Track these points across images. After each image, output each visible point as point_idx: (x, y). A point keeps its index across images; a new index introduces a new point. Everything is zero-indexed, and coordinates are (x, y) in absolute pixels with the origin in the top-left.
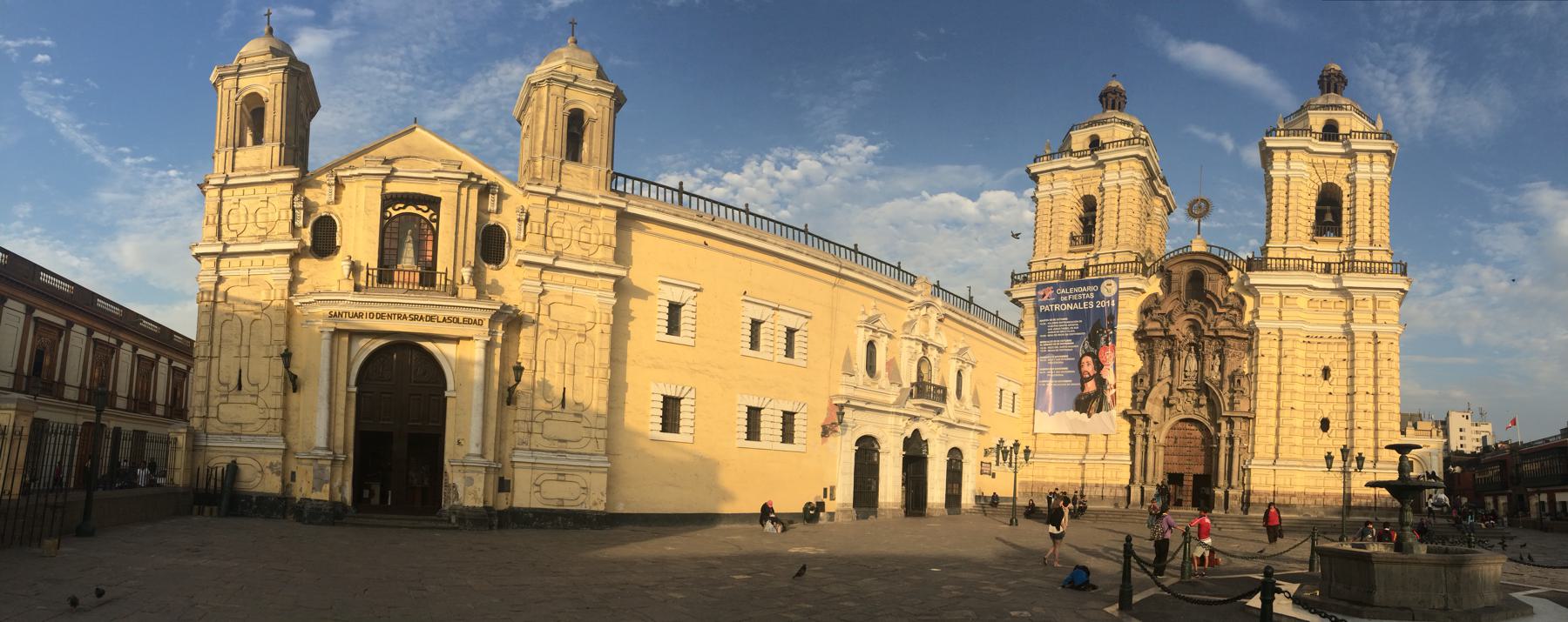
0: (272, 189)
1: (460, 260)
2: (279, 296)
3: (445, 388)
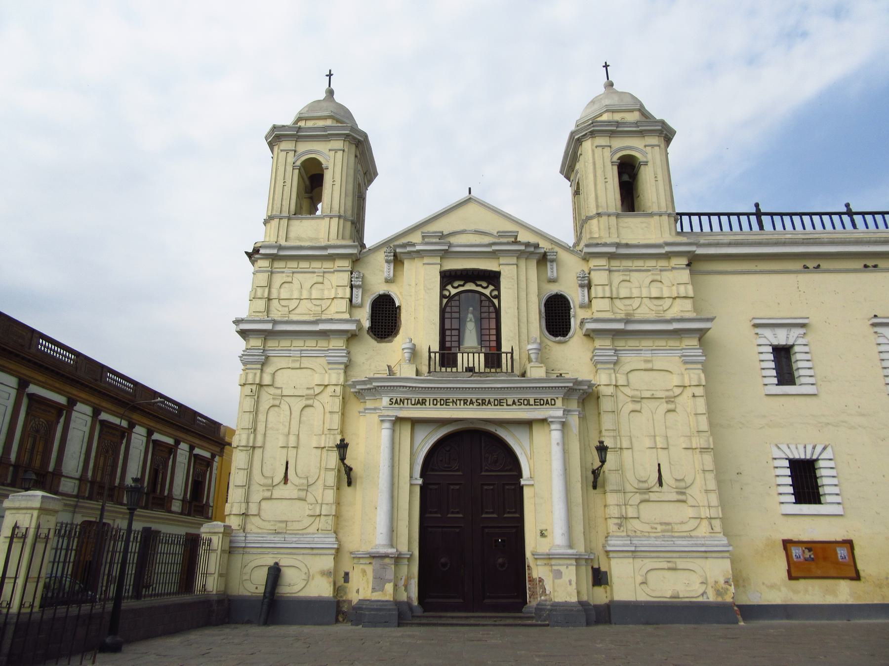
0: (328, 265)
1: (524, 337)
3: (520, 475)
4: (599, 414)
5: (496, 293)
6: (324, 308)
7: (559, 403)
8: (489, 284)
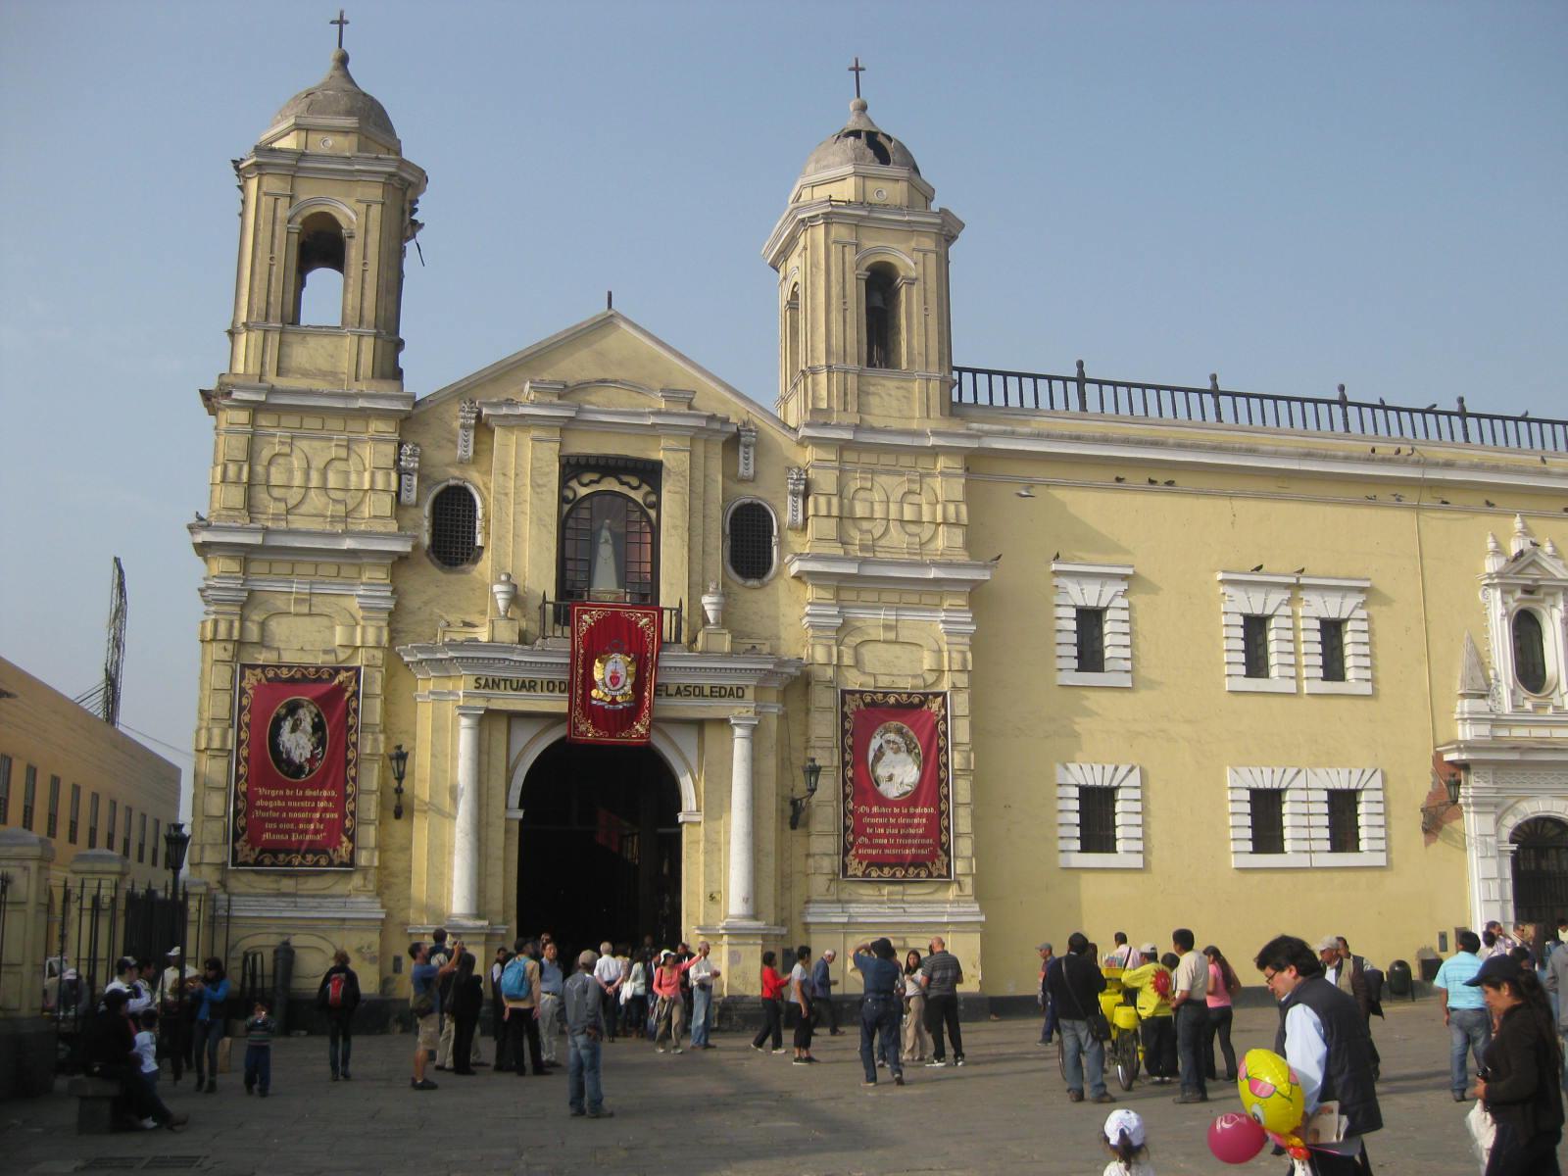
2: (371, 640)
4: (808, 712)
5: (653, 498)
6: (350, 507)
7: (750, 694)
8: (643, 481)
